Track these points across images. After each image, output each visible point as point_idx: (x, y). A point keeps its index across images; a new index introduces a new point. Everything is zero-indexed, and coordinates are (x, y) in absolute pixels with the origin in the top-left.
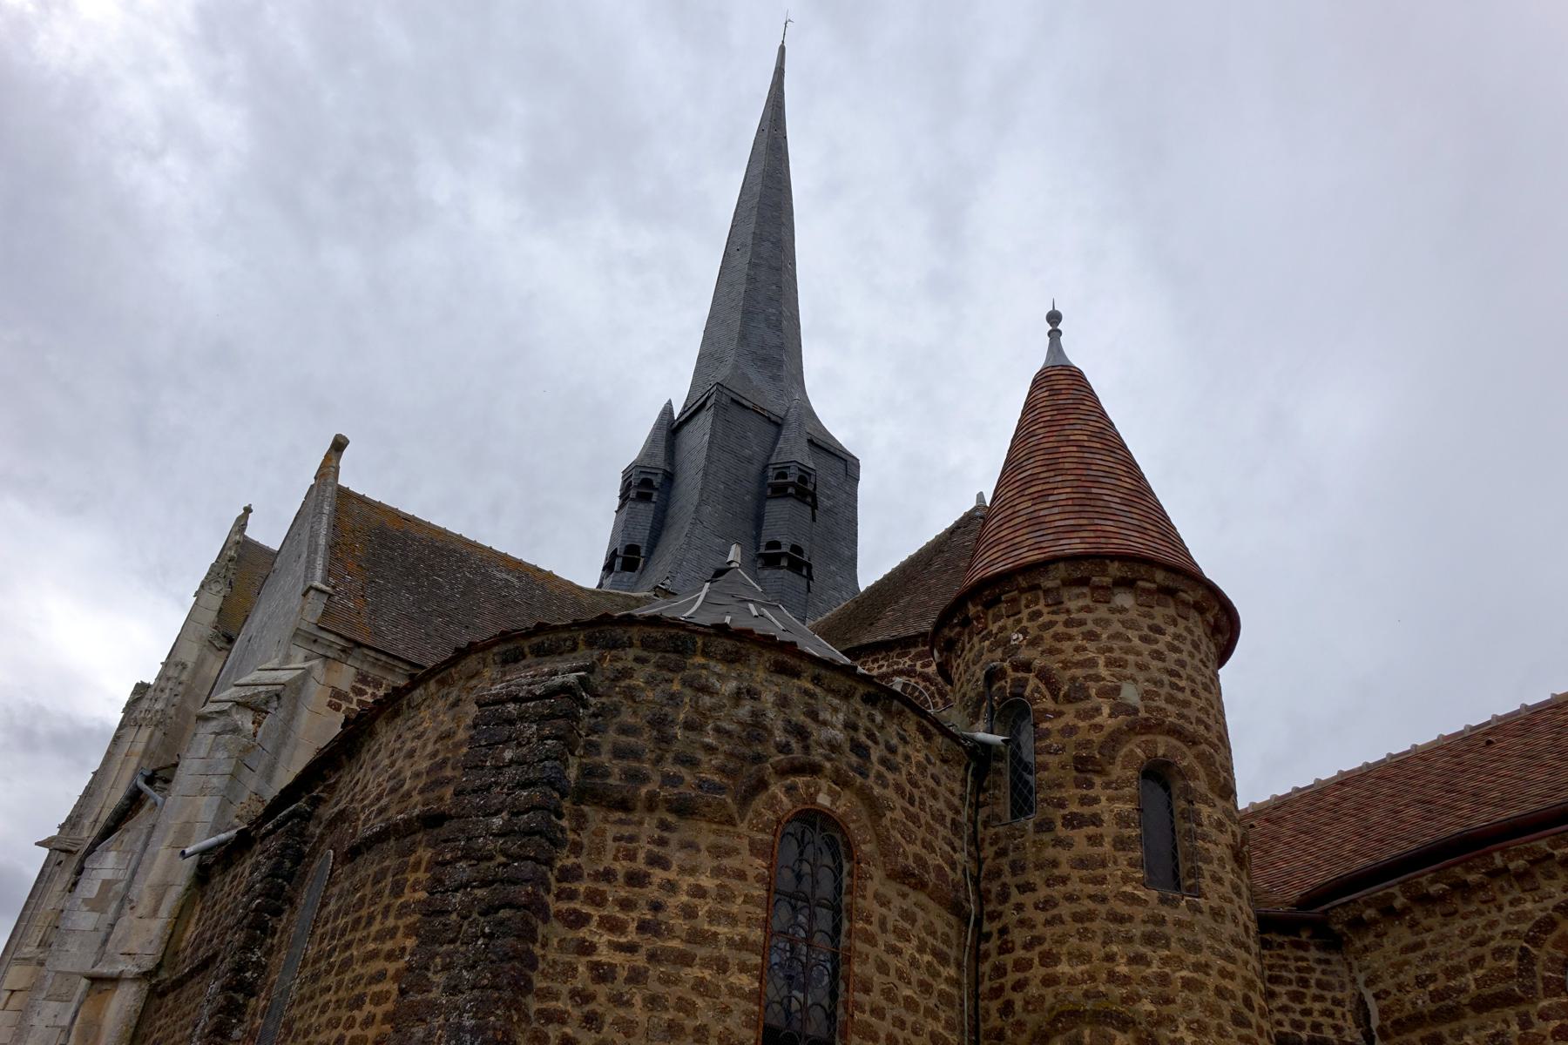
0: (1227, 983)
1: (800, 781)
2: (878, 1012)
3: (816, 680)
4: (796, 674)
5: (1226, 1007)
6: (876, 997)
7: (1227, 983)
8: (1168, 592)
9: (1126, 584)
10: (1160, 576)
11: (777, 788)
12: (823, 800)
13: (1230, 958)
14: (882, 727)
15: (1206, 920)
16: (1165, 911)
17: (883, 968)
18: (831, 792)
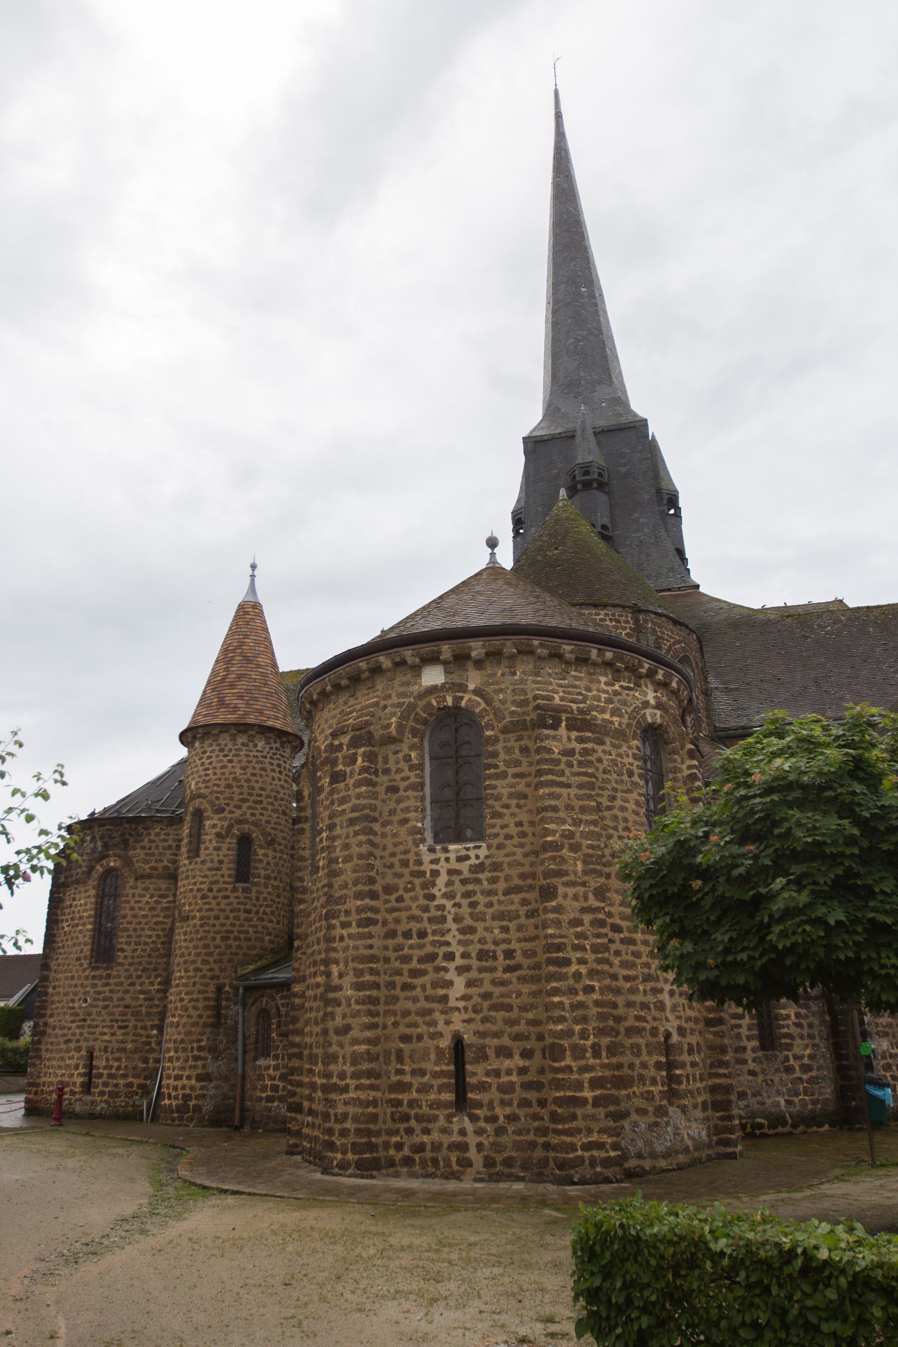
0: (203, 886)
1: (104, 862)
2: (130, 923)
3: (111, 824)
4: (104, 825)
5: (199, 895)
6: (129, 918)
7: (203, 886)
8: (209, 733)
9: (194, 738)
10: (200, 731)
11: (99, 868)
12: (112, 864)
13: (206, 876)
14: (135, 829)
15: (199, 866)
16: (190, 867)
17: (132, 909)
18: (115, 861)
